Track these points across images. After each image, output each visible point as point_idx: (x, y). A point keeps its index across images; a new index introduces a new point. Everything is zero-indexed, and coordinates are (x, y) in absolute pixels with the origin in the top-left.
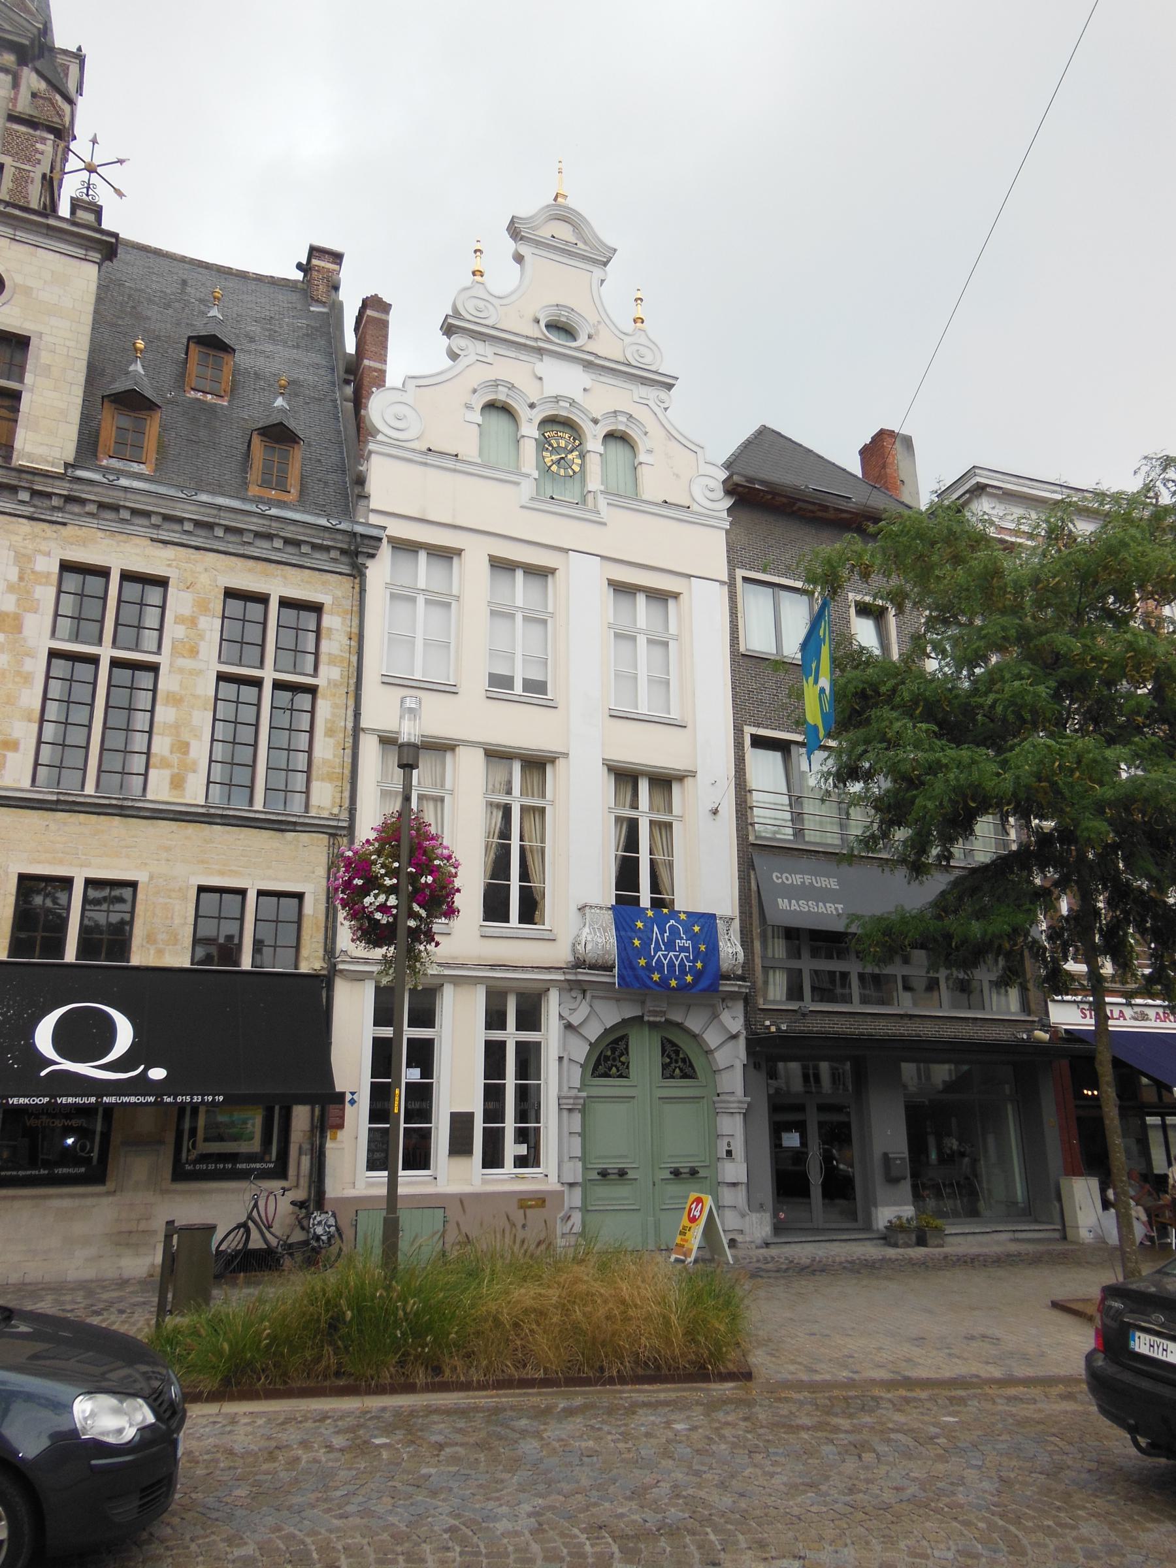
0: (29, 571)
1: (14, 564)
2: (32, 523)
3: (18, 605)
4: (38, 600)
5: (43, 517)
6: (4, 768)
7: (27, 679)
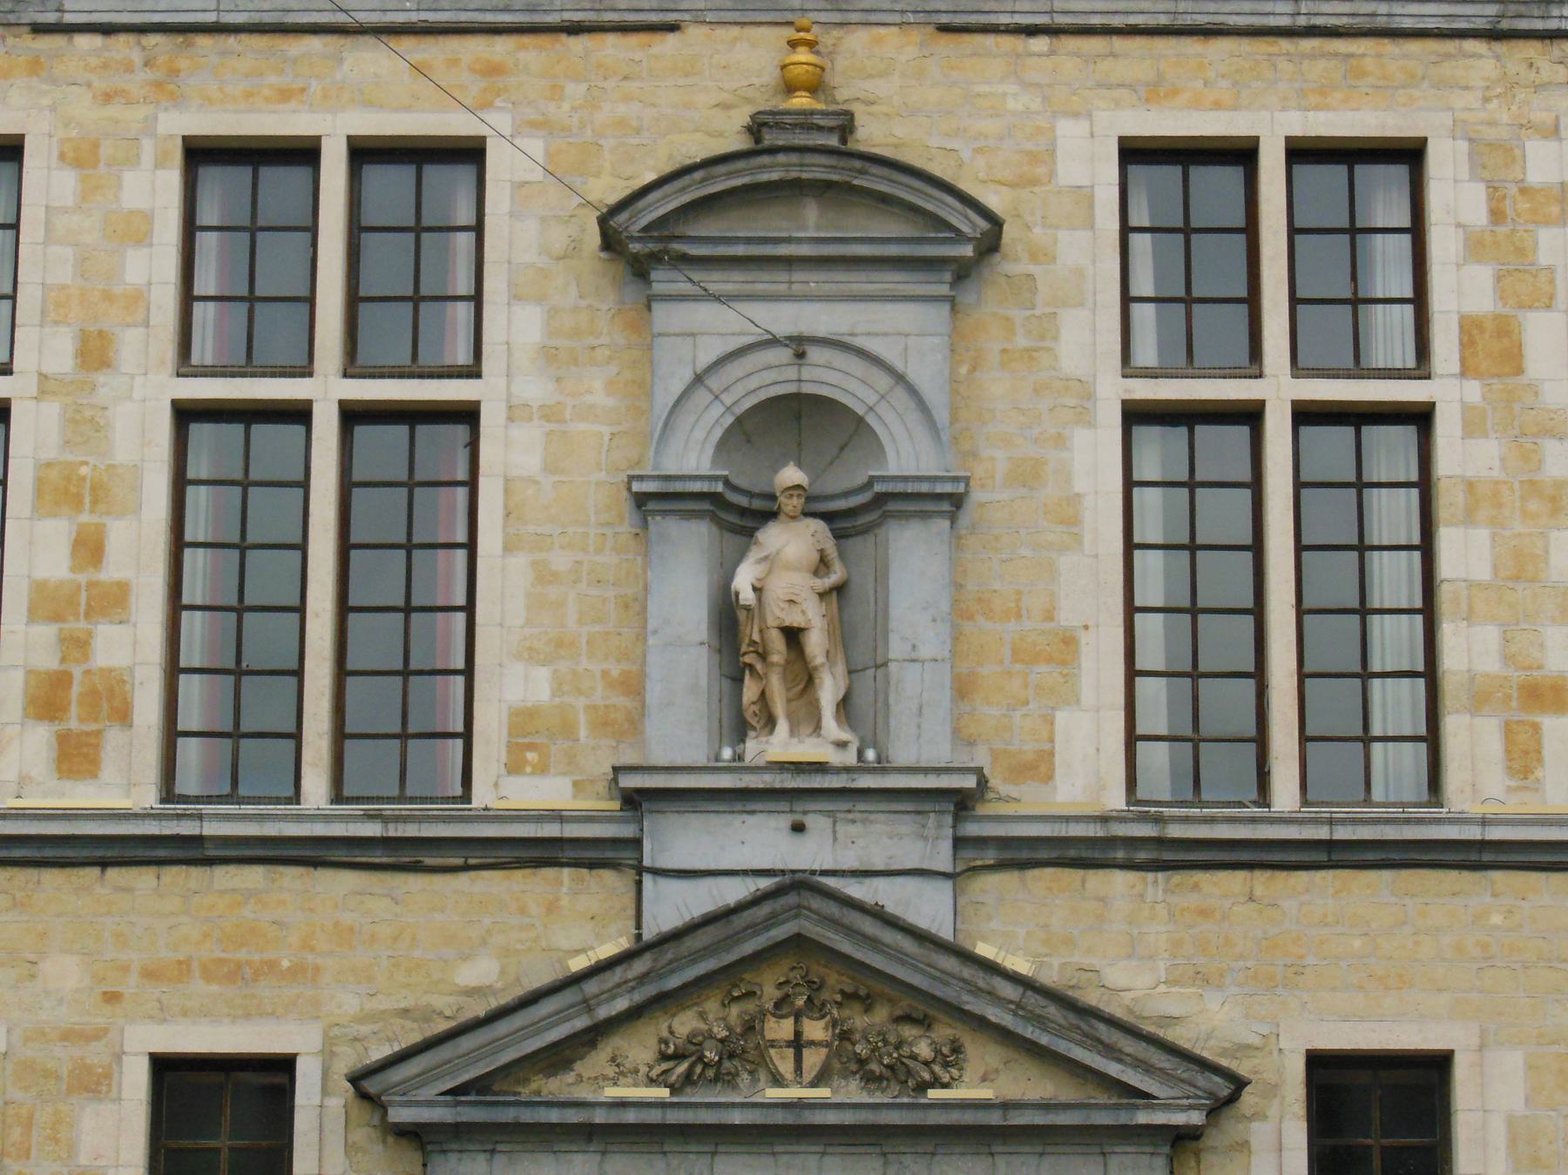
0: (1513, 190)
1: (1473, 177)
2: (1501, 47)
3: (1502, 295)
4: (1550, 269)
5: (1523, 25)
6: (1540, 760)
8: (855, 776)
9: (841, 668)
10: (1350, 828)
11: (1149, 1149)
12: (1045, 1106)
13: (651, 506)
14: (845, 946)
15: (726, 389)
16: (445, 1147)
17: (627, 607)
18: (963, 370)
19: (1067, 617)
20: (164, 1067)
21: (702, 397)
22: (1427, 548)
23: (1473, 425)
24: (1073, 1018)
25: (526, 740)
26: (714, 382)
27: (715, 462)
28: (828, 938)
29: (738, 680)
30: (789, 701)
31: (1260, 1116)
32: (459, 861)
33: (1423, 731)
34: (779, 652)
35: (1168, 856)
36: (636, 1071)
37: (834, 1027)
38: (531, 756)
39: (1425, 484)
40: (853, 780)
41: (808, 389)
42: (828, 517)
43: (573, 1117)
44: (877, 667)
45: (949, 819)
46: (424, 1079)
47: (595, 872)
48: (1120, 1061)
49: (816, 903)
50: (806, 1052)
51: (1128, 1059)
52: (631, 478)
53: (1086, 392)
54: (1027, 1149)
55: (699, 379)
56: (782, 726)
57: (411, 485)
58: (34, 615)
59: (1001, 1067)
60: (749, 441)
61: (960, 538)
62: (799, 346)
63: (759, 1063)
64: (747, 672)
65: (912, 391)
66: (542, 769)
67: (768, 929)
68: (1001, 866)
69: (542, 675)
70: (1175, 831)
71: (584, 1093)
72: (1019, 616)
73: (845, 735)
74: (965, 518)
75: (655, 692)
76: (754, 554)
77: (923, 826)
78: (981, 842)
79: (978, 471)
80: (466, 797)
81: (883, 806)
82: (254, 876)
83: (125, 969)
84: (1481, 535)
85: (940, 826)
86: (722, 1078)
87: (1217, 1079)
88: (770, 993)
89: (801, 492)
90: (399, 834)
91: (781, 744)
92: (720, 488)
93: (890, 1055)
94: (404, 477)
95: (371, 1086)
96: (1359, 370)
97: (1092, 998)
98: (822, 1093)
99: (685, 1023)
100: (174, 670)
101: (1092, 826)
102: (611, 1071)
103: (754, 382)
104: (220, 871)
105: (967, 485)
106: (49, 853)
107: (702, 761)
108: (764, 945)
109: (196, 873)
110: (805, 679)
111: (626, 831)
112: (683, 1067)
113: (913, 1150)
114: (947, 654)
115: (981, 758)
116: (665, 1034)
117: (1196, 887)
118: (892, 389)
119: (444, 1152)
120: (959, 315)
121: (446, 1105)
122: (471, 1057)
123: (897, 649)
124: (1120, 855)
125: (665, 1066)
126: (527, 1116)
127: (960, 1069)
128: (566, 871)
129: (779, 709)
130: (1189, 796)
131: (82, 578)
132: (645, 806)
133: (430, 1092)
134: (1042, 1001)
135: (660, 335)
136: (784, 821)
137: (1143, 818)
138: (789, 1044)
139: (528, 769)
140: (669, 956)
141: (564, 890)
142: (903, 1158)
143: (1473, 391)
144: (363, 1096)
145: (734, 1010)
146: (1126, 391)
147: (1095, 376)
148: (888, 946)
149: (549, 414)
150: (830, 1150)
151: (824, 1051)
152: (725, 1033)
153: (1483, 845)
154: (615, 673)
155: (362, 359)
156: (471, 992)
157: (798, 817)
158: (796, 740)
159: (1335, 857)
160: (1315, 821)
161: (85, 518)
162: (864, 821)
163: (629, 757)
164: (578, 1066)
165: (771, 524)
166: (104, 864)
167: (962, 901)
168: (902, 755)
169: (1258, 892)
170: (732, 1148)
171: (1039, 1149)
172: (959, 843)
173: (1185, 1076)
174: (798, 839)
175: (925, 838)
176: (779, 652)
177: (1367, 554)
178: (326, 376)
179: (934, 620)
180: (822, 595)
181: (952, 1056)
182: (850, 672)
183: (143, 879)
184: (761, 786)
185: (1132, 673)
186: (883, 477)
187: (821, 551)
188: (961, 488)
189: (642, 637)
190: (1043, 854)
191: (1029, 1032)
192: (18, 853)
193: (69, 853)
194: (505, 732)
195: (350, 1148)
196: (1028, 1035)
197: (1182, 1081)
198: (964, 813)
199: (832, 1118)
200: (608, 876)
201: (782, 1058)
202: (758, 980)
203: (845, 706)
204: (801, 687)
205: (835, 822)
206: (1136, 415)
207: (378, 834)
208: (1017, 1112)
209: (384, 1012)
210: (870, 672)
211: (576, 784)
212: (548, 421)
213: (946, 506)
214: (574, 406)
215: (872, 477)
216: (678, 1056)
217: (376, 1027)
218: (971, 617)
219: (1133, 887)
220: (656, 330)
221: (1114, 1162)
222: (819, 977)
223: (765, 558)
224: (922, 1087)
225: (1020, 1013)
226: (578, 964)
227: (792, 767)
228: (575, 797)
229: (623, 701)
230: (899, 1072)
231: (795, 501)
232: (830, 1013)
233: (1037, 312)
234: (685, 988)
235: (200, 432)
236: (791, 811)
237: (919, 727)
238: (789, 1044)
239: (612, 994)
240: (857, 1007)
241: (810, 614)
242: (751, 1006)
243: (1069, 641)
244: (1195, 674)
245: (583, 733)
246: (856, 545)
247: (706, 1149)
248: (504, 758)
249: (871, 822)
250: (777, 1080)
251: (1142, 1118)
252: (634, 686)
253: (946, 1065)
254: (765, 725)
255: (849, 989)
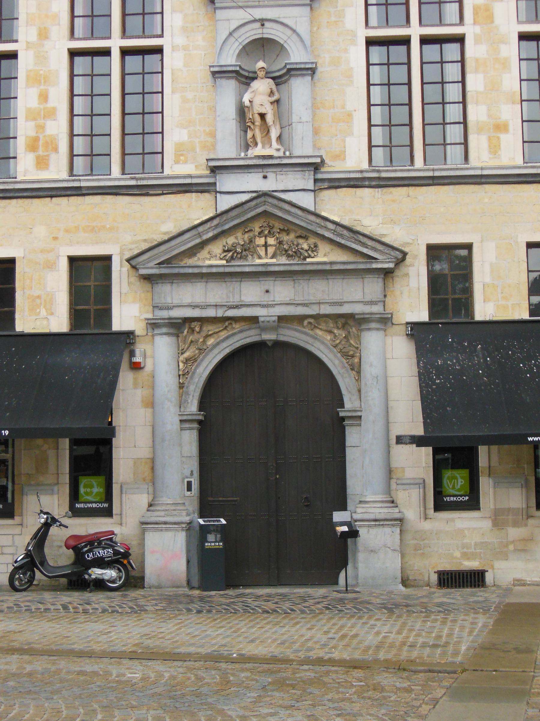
6: (500, 149)
7: (505, 64)
8: (282, 159)
9: (278, 127)
10: (439, 172)
11: (377, 276)
12: (344, 263)
13: (217, 75)
14: (280, 214)
15: (240, 37)
16: (158, 282)
17: (211, 109)
18: (315, 29)
19: (349, 107)
20: (72, 260)
21: (232, 40)
22: (463, 82)
23: (478, 40)
24: (352, 235)
25: (181, 153)
26: (236, 35)
27: (236, 61)
28: (275, 211)
29: (246, 132)
30: (262, 138)
31: (412, 265)
32: (161, 192)
33: (463, 141)
34: (258, 122)
35: (382, 183)
36: (216, 256)
37: (277, 240)
38: (182, 158)
39: (462, 62)
40: (282, 161)
41: (265, 36)
42: (273, 78)
43: (196, 271)
44: (289, 125)
45: (312, 173)
46: (149, 260)
47: (203, 194)
48: (367, 248)
49: (270, 200)
50: (268, 248)
51: (369, 247)
52: (210, 66)
53: (354, 35)
54: (339, 277)
55: (231, 34)
56: (260, 145)
57: (143, 74)
58: (27, 119)
59: (330, 251)
60: (248, 54)
61: (315, 83)
62: (262, 22)
63: (254, 253)
64: (249, 129)
65: (298, 35)
66: (185, 162)
67: (255, 209)
68: (330, 188)
69: (185, 132)
70: (384, 175)
71: (200, 263)
72: (334, 107)
73: (279, 147)
74: (316, 76)
75: (219, 135)
76: (250, 90)
77: (304, 175)
78: (323, 180)
79: (320, 62)
80: (163, 172)
81: (291, 169)
82: (98, 199)
83: (59, 230)
84: (480, 76)
85: (310, 175)
86: (243, 257)
87: (397, 253)
88: (257, 230)
89: (264, 70)
90: (141, 184)
91: (259, 150)
92: (238, 68)
93: (295, 248)
94: (141, 71)
95: (133, 263)
96: (441, 23)
97: (358, 228)
98: (274, 261)
99: (231, 240)
100: (72, 135)
101: (357, 174)
102: (208, 256)
103: (248, 35)
104: (87, 198)
105: (316, 65)
106: (34, 194)
107: (233, 156)
108: (255, 214)
109: (80, 198)
110: (266, 130)
111: (211, 180)
112: (231, 253)
113: (302, 278)
114: (311, 120)
115: (322, 153)
116: (225, 244)
117: (391, 193)
118: (292, 35)
119: (157, 283)
120: (313, 11)
121: (157, 268)
122: (165, 252)
123: (295, 119)
124: (367, 183)
125: (225, 254)
126: (182, 271)
127: (317, 253)
128: (194, 194)
129: (259, 140)
130: (389, 164)
131: (42, 107)
132: (217, 172)
133: (152, 264)
134: (342, 229)
135: (218, 20)
136: (261, 175)
137: (373, 171)
138: (263, 246)
139: (181, 162)
140: (225, 219)
141: (193, 200)
142: (300, 281)
143: (478, 29)
144: (134, 267)
145: (246, 236)
146: (367, 33)
147: (357, 29)
148: (293, 213)
149: (185, 48)
150: (277, 279)
151: (274, 247)
152: (243, 243)
153: (482, 176)
154: (207, 130)
155: (127, 33)
156: (165, 233)
157: (265, 174)
158: (263, 149)
159: (435, 182)
160: (428, 170)
161: (42, 87)
162: (285, 174)
163: (212, 156)
164: (198, 255)
165: (255, 81)
166: (52, 197)
167: (317, 199)
168: (296, 153)
169: (411, 194)
170: (246, 279)
171: (343, 277)
172: (316, 181)
173: (387, 252)
174: (265, 180)
175: (305, 179)
176: (258, 122)
177: (444, 85)
178: (115, 39)
179: (306, 109)
180: (271, 103)
181: (314, 248)
182: (281, 128)
183: (63, 201)
184: (253, 164)
185: (370, 126)
186: (289, 63)
187: (271, 89)
188: (314, 66)
189: (215, 119)
190: (343, 184)
191: (338, 239)
192: (25, 194)
193: (41, 194)
194: (174, 151)
195: (129, 283)
196: (338, 240)
197: (387, 253)
198: (317, 171)
199: (277, 269)
200: (206, 195)
201: (261, 250)
202: (254, 226)
203: (279, 138)
204: (266, 133)
205: (276, 175)
206: (370, 42)
207: (135, 184)
208: (335, 265)
209: (138, 241)
210: (287, 127)
211: (196, 166)
212: (185, 50)
213: (310, 72)
214: (193, 45)
215: (286, 63)
216: (228, 251)
217: (136, 245)
218: (319, 109)
219: (371, 193)
220: (217, 19)
221: (366, 280)
222: (272, 224)
223: (253, 91)
224: (305, 259)
225: (335, 233)
226: (197, 222)
227: (262, 157)
228: (196, 170)
229: (210, 139)
230: (298, 254)
231: (262, 73)
232: (276, 235)
233: (338, 9)
234: (230, 229)
235: (77, 59)
236: (263, 172)
237: (302, 144)
238: (263, 246)
239: (207, 231)
240: (285, 234)
241: (268, 109)
242: (251, 234)
243: (350, 115)
244: (390, 125)
245: (198, 150)
246: (282, 87)
247: (239, 280)
248: (174, 159)
249: (288, 175)
250: (260, 257)
251: (374, 266)
252: (213, 135)
253: (313, 251)
254: (255, 146)
255: (282, 228)
